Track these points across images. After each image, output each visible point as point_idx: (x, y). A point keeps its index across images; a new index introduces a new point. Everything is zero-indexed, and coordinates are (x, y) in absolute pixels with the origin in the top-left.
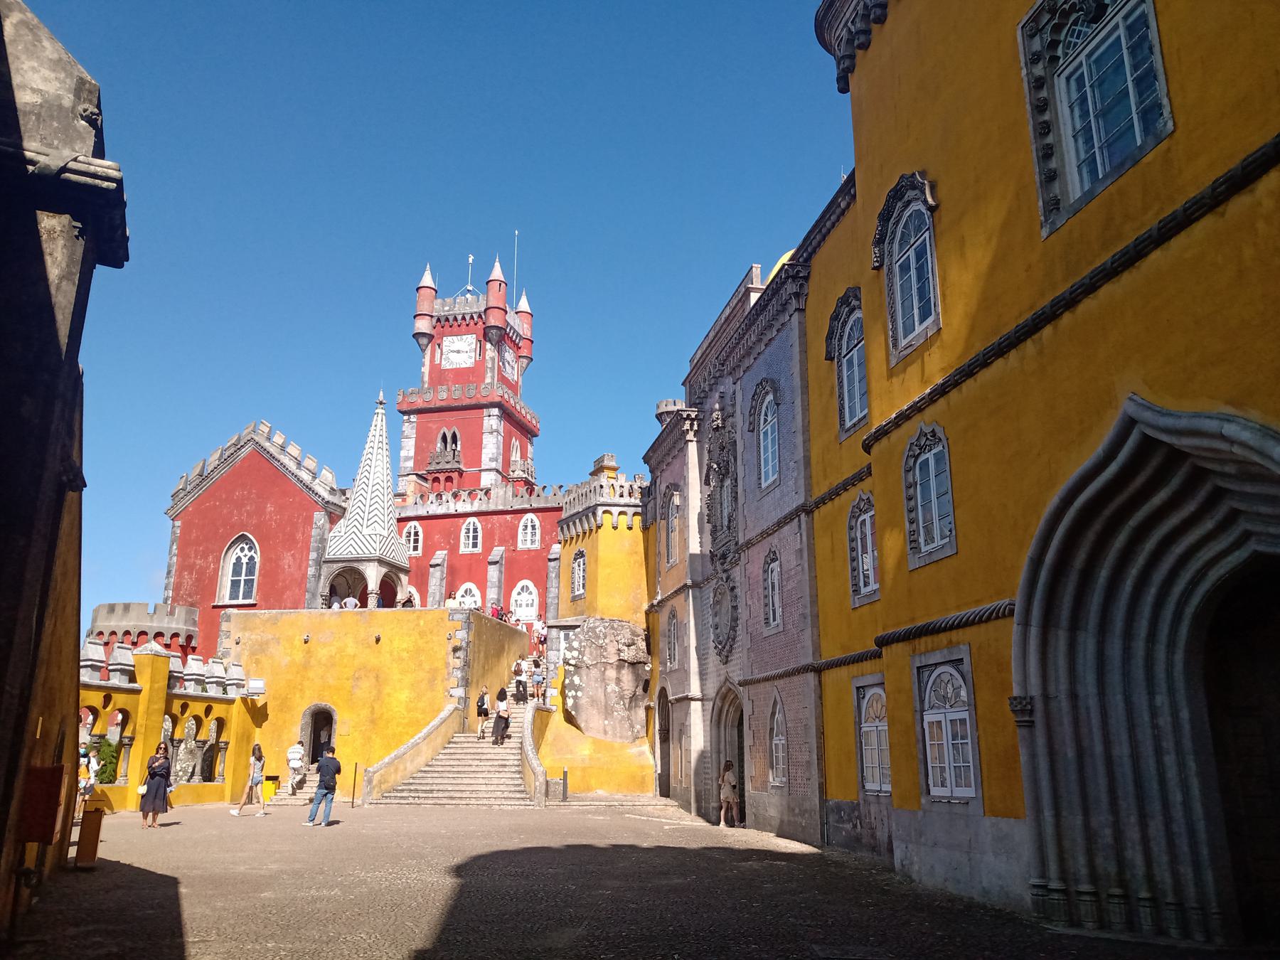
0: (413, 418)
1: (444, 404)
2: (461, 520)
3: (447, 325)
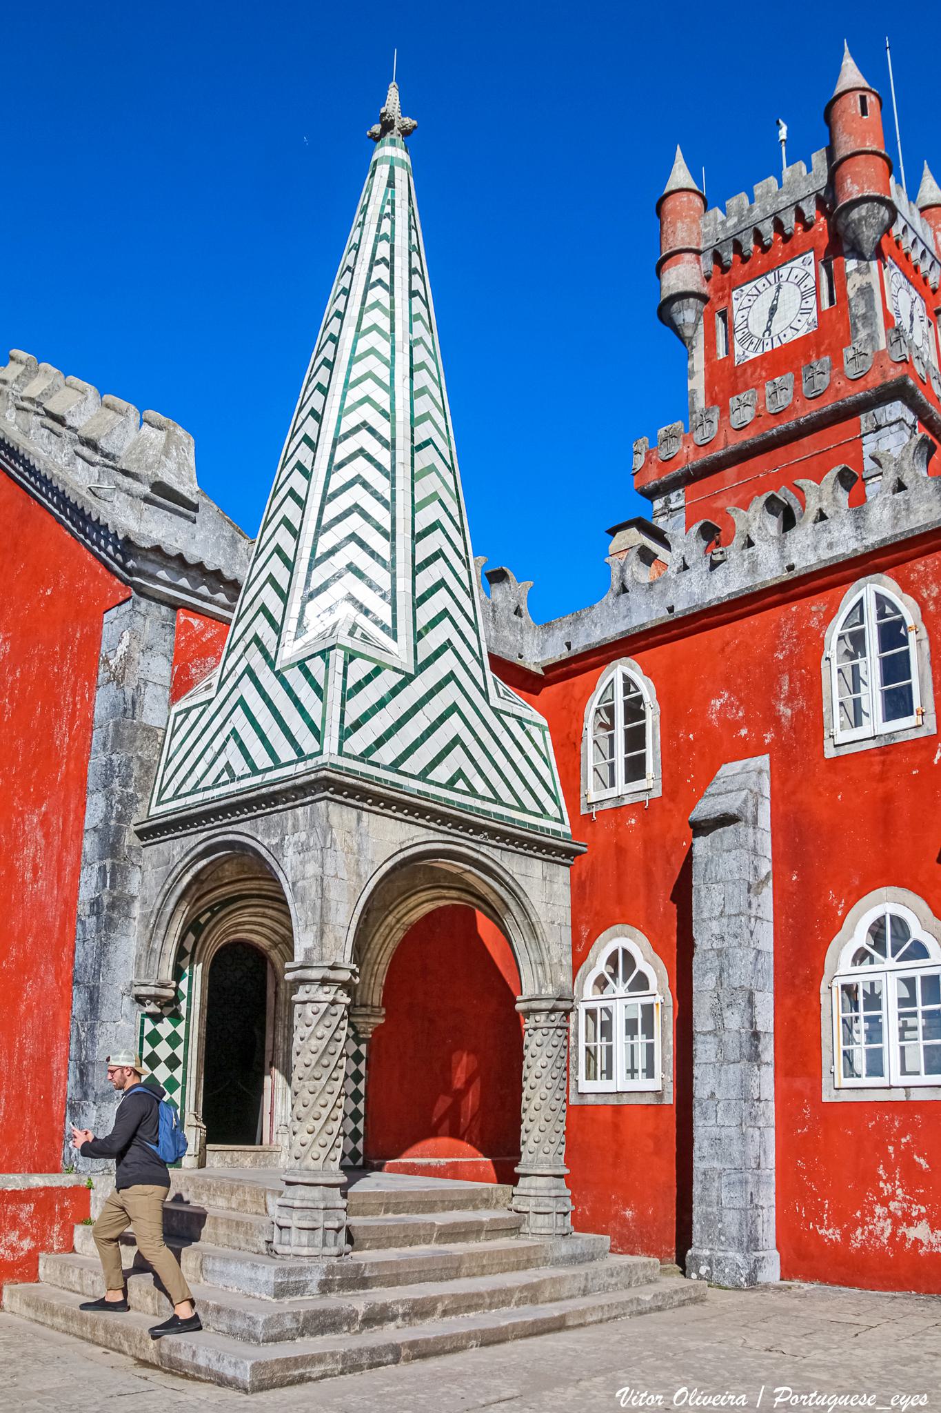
0: (677, 499)
1: (748, 437)
2: (817, 605)
3: (738, 261)
